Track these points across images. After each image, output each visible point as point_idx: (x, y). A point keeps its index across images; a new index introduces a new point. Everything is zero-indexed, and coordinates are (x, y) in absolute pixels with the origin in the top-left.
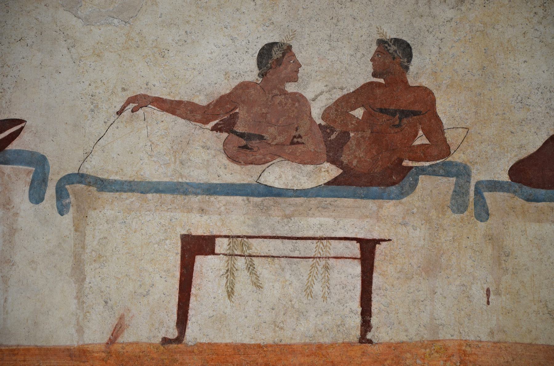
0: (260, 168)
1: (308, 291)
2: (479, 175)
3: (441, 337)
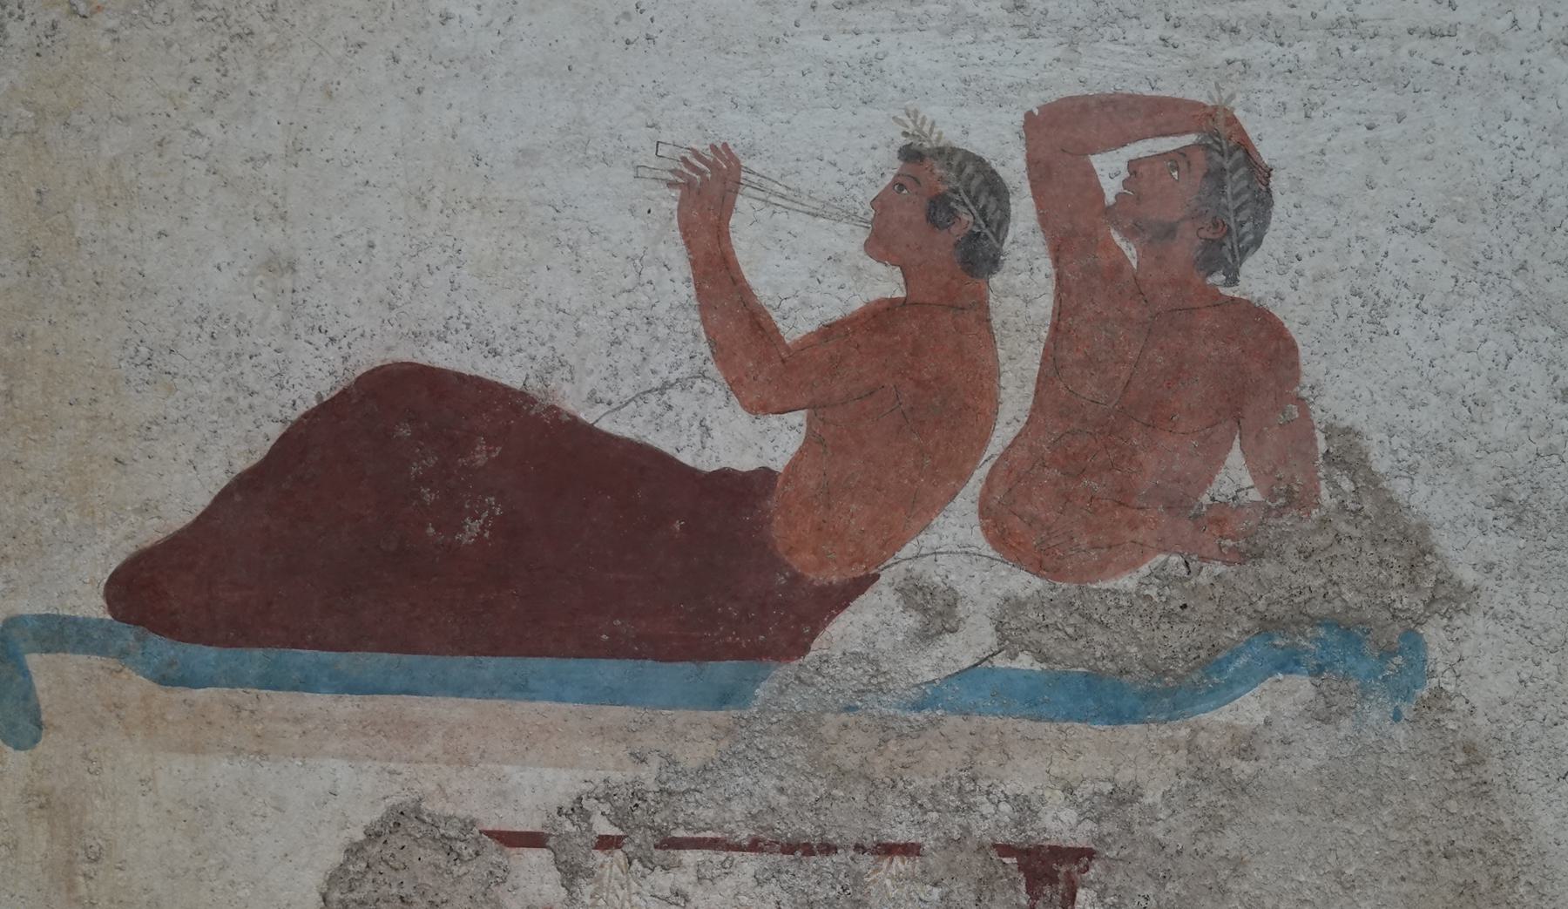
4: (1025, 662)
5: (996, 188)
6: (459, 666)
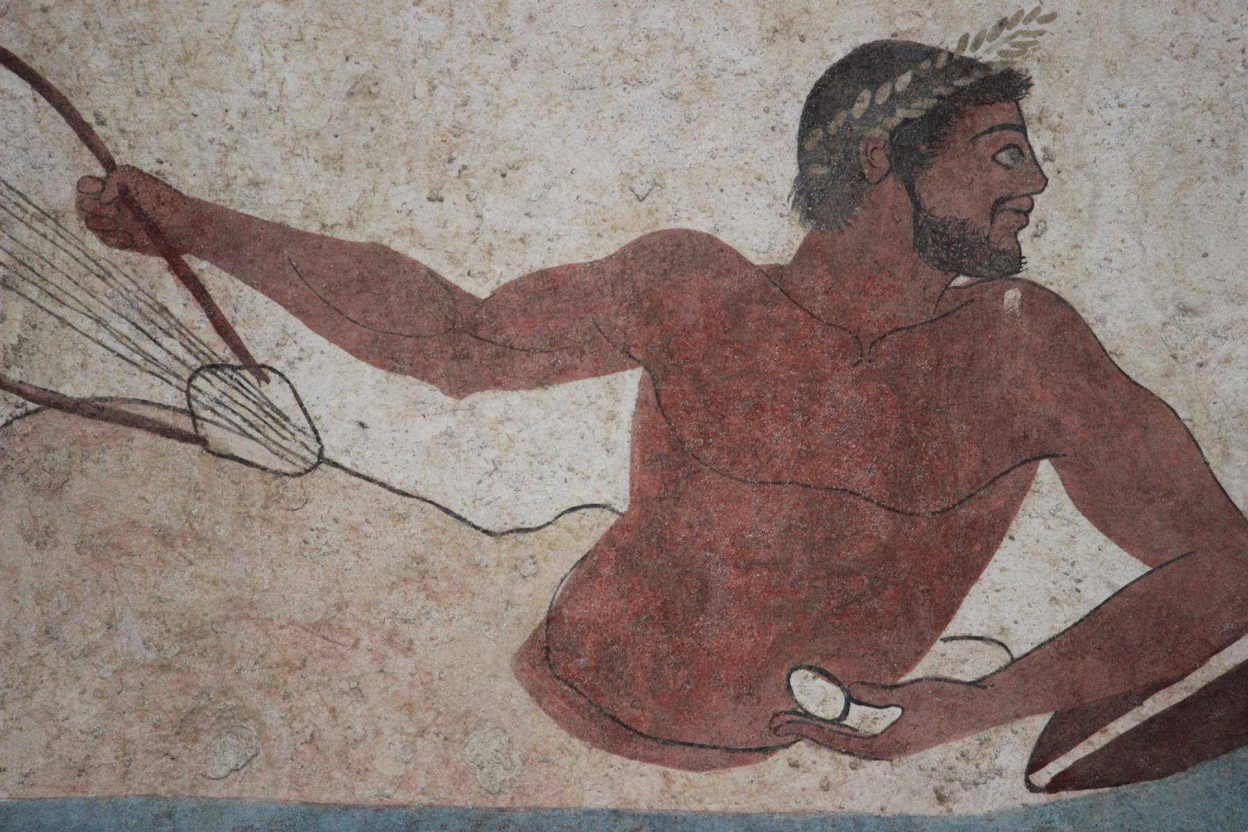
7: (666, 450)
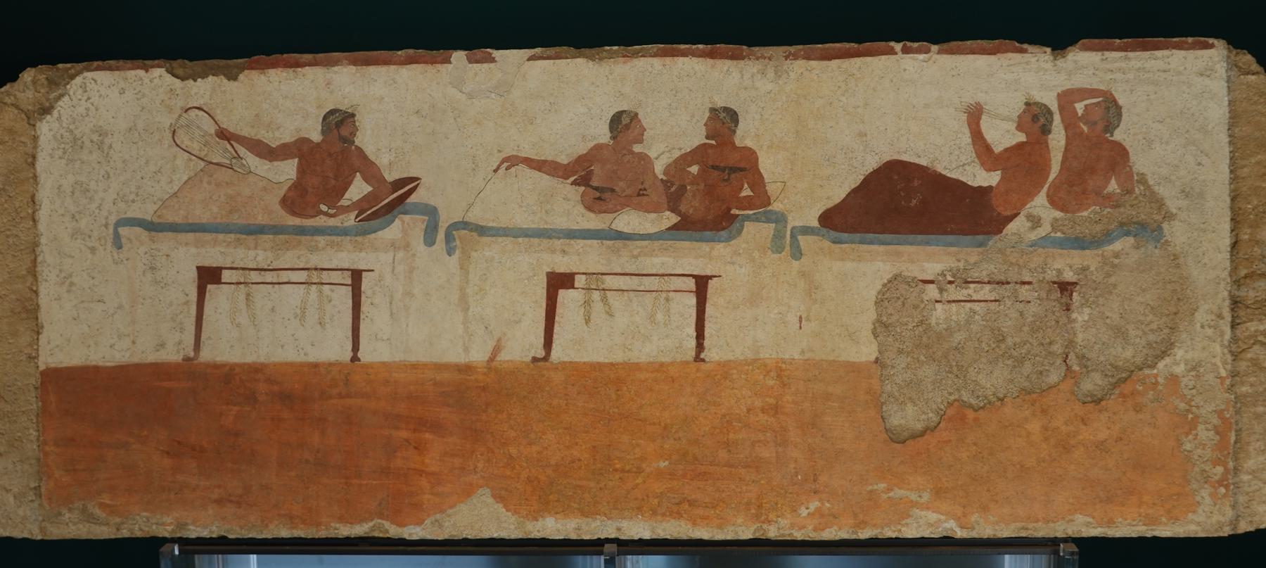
0: (611, 216)
1: (651, 318)
2: (794, 221)
3: (762, 356)
4: (1059, 234)
5: (1050, 112)
6: (911, 237)
7: (301, 171)
